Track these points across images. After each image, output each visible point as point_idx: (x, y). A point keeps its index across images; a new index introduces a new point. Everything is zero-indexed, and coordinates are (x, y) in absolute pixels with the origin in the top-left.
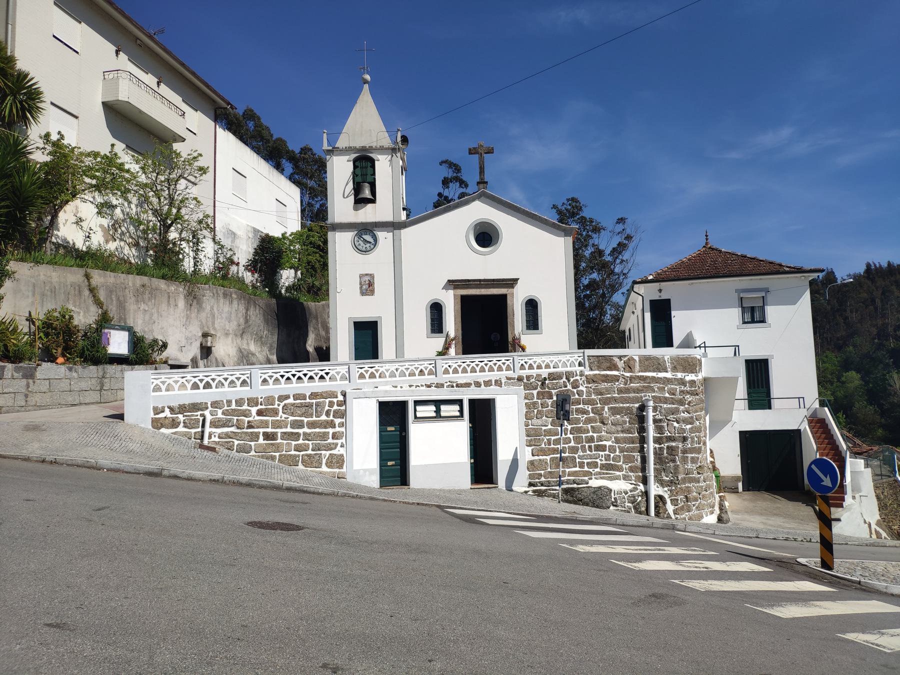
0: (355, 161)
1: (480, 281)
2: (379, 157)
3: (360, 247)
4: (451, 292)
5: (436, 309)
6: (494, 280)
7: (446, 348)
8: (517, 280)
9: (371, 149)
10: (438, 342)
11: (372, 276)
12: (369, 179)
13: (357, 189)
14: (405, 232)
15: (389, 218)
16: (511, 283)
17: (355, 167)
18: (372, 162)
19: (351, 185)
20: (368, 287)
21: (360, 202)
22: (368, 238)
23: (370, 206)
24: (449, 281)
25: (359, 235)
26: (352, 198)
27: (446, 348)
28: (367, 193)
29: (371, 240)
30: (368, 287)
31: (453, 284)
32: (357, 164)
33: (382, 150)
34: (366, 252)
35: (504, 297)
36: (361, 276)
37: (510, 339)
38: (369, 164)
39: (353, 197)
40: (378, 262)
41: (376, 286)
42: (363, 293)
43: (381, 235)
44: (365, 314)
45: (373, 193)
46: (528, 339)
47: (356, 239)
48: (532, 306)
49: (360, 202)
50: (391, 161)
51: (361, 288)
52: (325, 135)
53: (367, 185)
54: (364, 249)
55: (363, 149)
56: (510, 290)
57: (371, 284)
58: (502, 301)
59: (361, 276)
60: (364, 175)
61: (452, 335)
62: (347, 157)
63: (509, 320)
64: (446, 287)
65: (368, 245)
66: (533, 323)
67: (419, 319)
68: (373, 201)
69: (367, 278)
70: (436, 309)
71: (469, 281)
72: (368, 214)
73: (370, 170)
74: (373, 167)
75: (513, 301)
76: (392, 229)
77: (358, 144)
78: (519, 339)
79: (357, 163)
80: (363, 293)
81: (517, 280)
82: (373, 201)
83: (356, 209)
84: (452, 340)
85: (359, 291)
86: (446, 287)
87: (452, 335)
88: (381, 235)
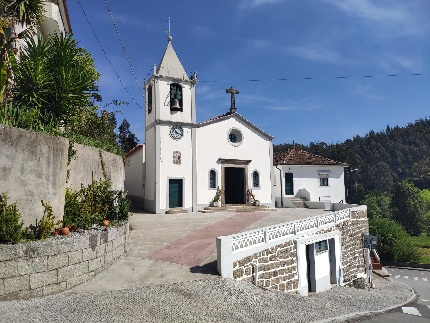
0: (171, 85)
1: (234, 160)
2: (185, 86)
3: (173, 136)
4: (220, 165)
5: (213, 174)
6: (240, 160)
8: (250, 161)
9: (181, 80)
10: (213, 193)
11: (180, 153)
12: (179, 97)
13: (172, 102)
14: (199, 130)
15: (189, 121)
17: (171, 89)
18: (181, 88)
19: (169, 99)
20: (178, 160)
21: (174, 110)
22: (178, 131)
23: (179, 113)
24: (220, 160)
25: (173, 129)
29: (180, 132)
30: (178, 160)
31: (221, 161)
33: (186, 82)
34: (176, 139)
36: (174, 153)
38: (179, 89)
39: (169, 106)
40: (183, 145)
41: (182, 159)
42: (175, 163)
43: (185, 130)
44: (176, 176)
45: (181, 105)
46: (255, 192)
48: (256, 174)
49: (174, 110)
50: (191, 89)
51: (174, 159)
54: (175, 137)
55: (176, 80)
57: (179, 158)
59: (174, 153)
60: (176, 95)
61: (220, 188)
62: (167, 82)
64: (218, 162)
65: (178, 135)
66: (256, 184)
67: (204, 179)
68: (181, 110)
69: (177, 154)
70: (213, 174)
71: (229, 160)
72: (178, 117)
73: (179, 93)
74: (181, 90)
76: (191, 127)
77: (174, 76)
79: (172, 87)
80: (175, 163)
81: (250, 161)
82: (181, 110)
83: (171, 113)
85: (173, 161)
86: (218, 162)
87: (220, 188)
88: (185, 130)
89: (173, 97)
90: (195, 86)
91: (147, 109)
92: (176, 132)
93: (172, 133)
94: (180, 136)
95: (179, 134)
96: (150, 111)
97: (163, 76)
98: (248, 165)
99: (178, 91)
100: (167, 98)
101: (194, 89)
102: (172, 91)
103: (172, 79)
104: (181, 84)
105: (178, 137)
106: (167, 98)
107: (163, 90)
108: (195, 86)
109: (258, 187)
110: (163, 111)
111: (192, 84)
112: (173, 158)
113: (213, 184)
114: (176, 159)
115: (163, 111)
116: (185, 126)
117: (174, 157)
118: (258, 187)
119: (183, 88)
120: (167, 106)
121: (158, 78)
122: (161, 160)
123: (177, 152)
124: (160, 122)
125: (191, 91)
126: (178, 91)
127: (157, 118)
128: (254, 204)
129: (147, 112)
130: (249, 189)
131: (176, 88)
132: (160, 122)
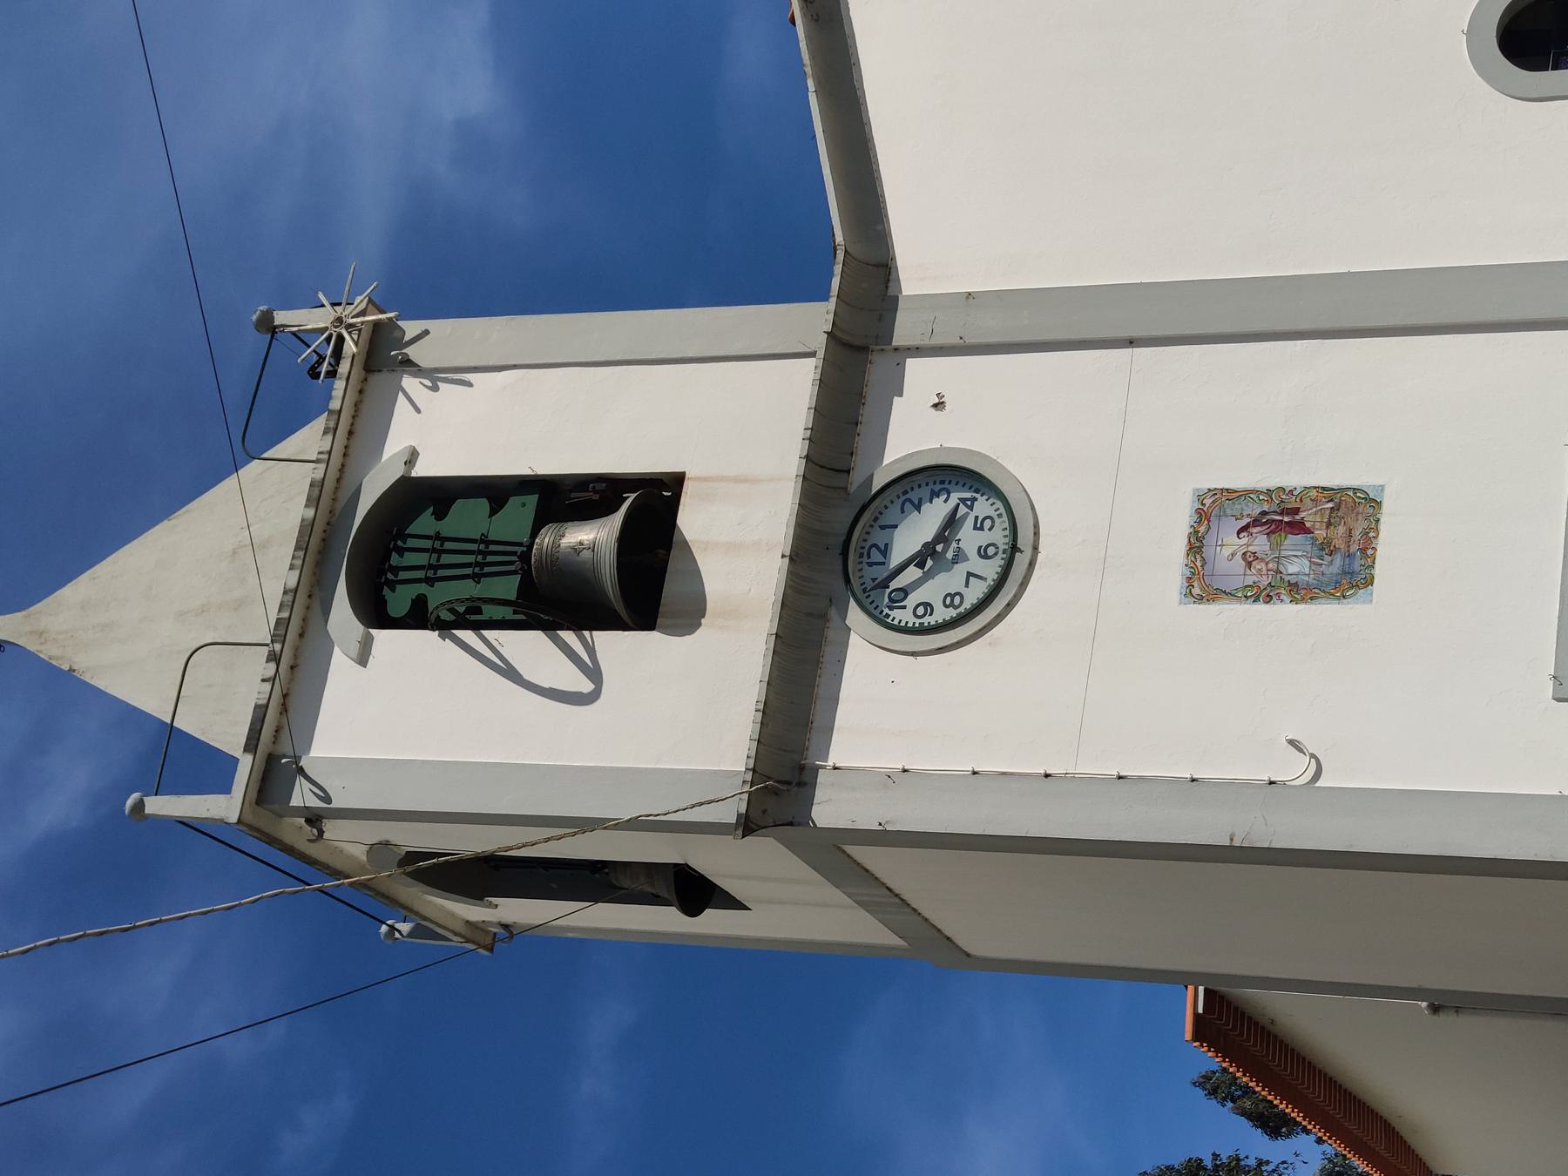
0: (375, 614)
2: (394, 446)
9: (332, 497)
11: (1212, 508)
13: (561, 603)
15: (793, 388)
17: (418, 618)
19: (529, 649)
20: (1303, 541)
22: (914, 532)
23: (691, 521)
25: (879, 597)
26: (615, 647)
28: (593, 538)
29: (933, 514)
30: (1303, 541)
32: (399, 601)
33: (360, 431)
36: (1202, 585)
38: (425, 523)
39: (609, 643)
41: (1296, 477)
42: (1349, 573)
43: (910, 433)
47: (903, 616)
50: (434, 377)
51: (1299, 592)
52: (158, 805)
53: (545, 539)
54: (990, 570)
55: (316, 548)
57: (1281, 516)
59: (1202, 585)
60: (485, 557)
62: (340, 663)
65: (969, 539)
69: (1228, 545)
74: (440, 494)
76: (878, 367)
77: (279, 572)
79: (399, 601)
80: (1349, 573)
83: (690, 616)
85: (1323, 614)
88: (910, 433)
89: (508, 587)
90: (411, 328)
91: (665, 920)
92: (927, 556)
93: (941, 614)
94: (983, 507)
95: (952, 522)
96: (693, 891)
97: (260, 713)
99: (449, 526)
100: (510, 673)
101: (438, 339)
102: (437, 596)
103: (308, 602)
104: (373, 488)
105: (999, 536)
106: (510, 673)
107: (428, 723)
108: (411, 328)
110: (656, 721)
111: (383, 356)
112: (1284, 611)
114: (1297, 567)
115: (656, 721)
116: (862, 443)
117: (1264, 595)
119: (420, 471)
120: (594, 673)
121: (277, 770)
122: (1295, 770)
123: (1196, 546)
124: (783, 776)
125: (457, 374)
126: (449, 526)
127: (728, 813)
129: (713, 922)
131: (423, 558)
132: (783, 776)
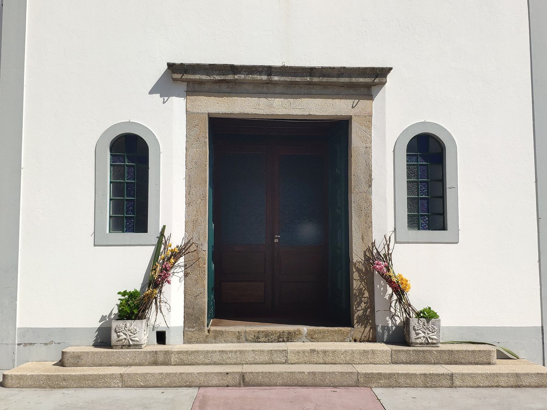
1: (269, 70)
4: (178, 105)
5: (130, 155)
6: (311, 71)
7: (155, 281)
8: (381, 74)
16: (366, 82)
27: (155, 281)
35: (340, 128)
37: (357, 255)
48: (427, 155)
56: (363, 103)
58: (334, 137)
63: (355, 199)
66: (429, 207)
70: (130, 155)
71: (234, 69)
75: (368, 140)
78: (387, 257)
81: (381, 74)
84: (176, 255)
98: (370, 97)
109: (444, 227)
113: (130, 208)
118: (444, 227)
128: (401, 337)
130: (378, 237)
